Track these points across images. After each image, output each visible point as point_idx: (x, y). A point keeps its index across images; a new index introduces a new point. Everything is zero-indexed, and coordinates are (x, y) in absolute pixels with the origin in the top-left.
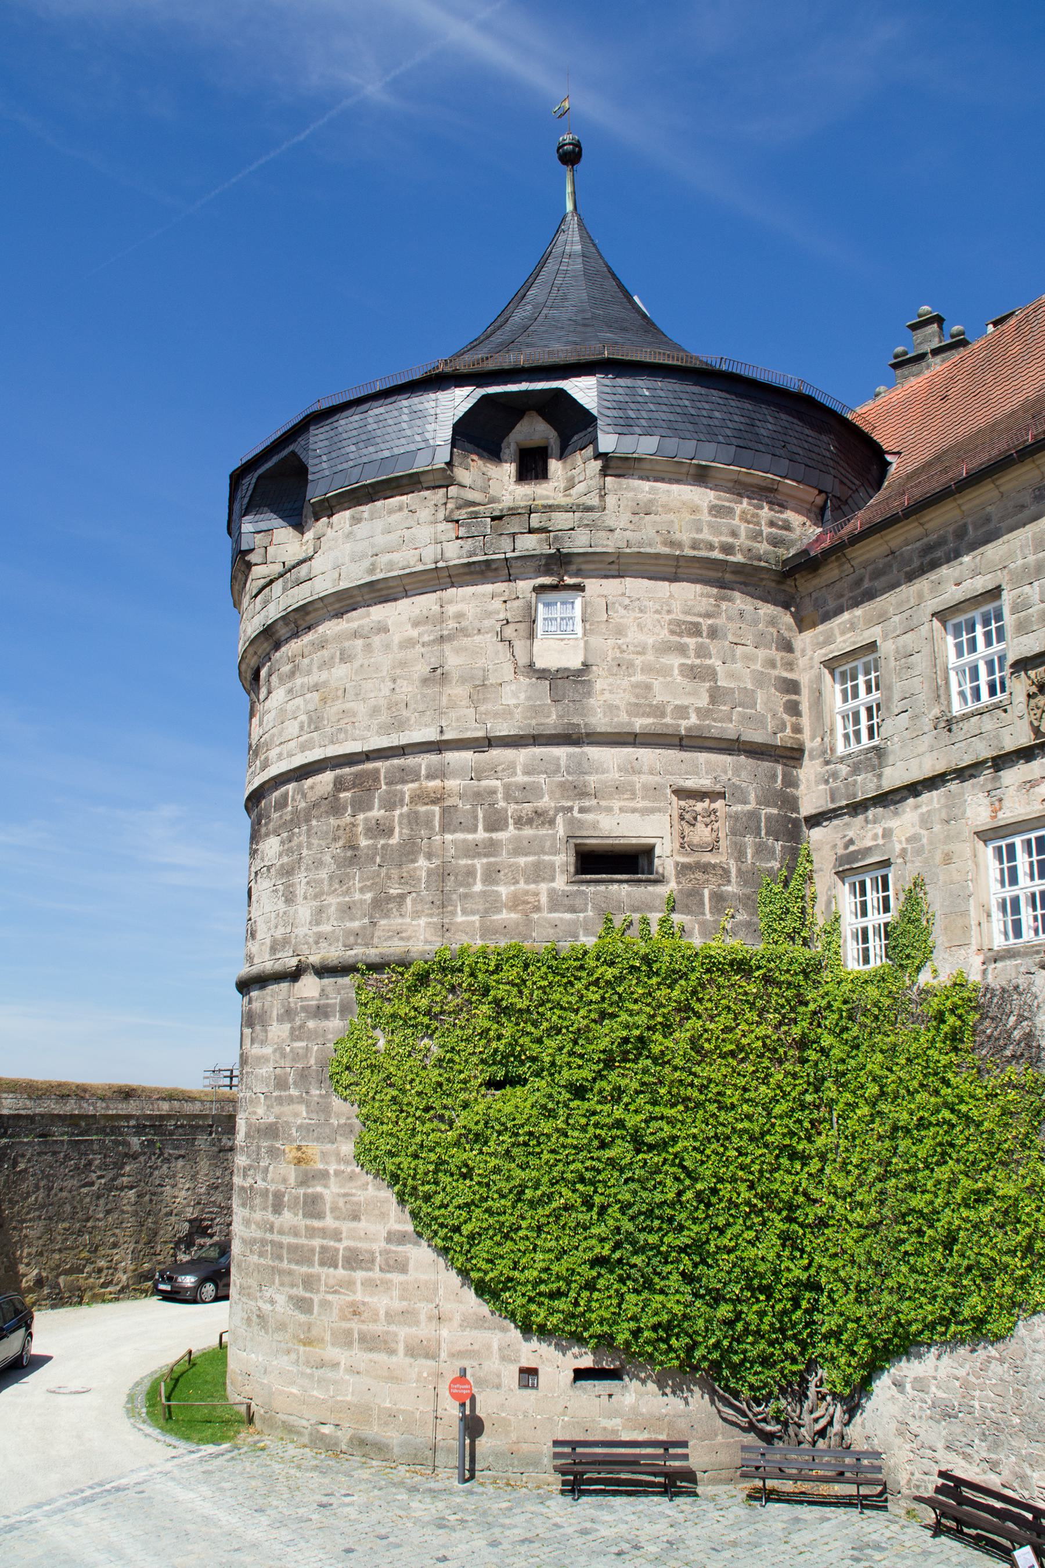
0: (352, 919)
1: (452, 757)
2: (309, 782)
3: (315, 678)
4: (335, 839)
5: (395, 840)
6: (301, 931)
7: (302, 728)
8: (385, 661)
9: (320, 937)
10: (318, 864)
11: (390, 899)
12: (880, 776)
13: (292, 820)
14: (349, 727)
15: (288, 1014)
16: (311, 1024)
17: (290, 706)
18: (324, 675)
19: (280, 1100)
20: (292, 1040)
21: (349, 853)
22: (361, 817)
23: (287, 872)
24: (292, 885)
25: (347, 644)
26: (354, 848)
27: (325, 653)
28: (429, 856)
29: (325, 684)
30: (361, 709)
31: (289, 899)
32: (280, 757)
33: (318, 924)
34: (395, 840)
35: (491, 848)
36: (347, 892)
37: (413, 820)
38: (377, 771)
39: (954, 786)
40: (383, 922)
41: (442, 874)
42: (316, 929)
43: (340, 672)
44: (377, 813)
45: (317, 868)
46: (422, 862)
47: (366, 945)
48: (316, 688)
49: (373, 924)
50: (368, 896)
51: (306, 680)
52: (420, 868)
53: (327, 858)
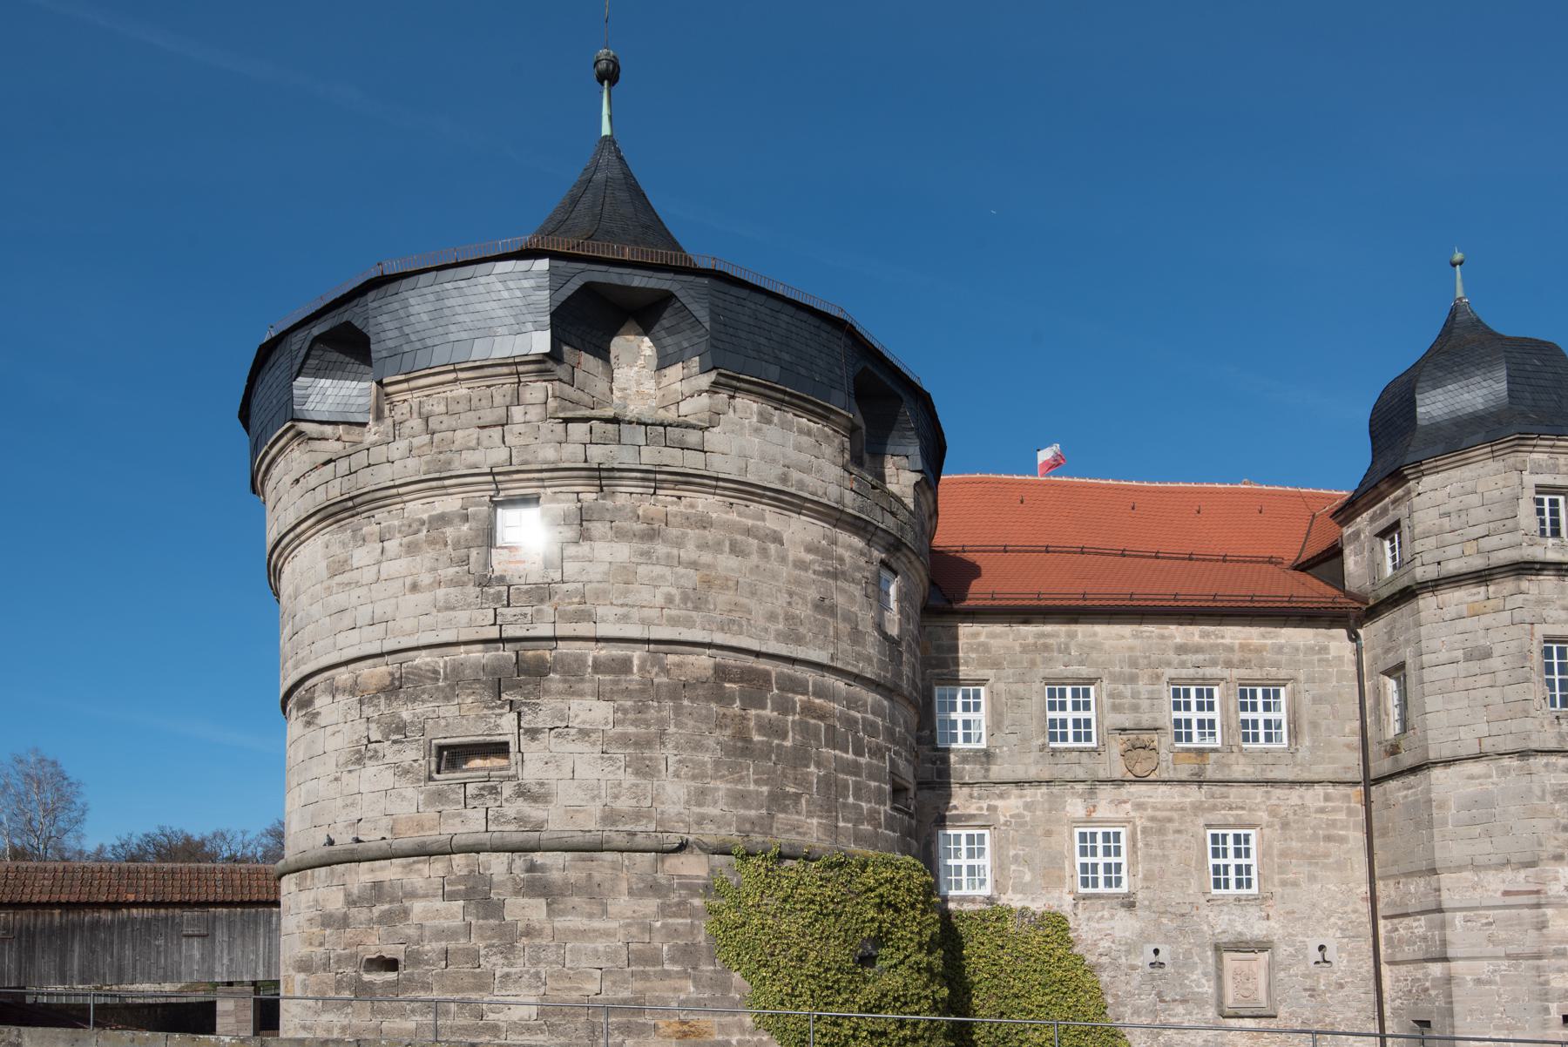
0: (748, 807)
1: (831, 680)
2: (671, 658)
3: (689, 552)
4: (720, 726)
5: (788, 743)
6: (672, 810)
7: (669, 599)
8: (785, 571)
9: (700, 821)
10: (699, 747)
11: (786, 795)
12: (987, 770)
13: (643, 691)
14: (744, 623)
15: (654, 889)
16: (697, 902)
17: (641, 570)
18: (706, 557)
19: (645, 976)
20: (664, 916)
21: (740, 744)
22: (753, 712)
23: (643, 743)
24: (651, 759)
25: (739, 537)
26: (748, 740)
27: (710, 535)
28: (818, 765)
29: (709, 566)
30: (758, 610)
31: (644, 769)
32: (625, 618)
33: (700, 805)
34: (788, 743)
35: (854, 769)
36: (740, 780)
37: (803, 728)
38: (767, 674)
39: (1056, 790)
40: (781, 816)
41: (827, 783)
42: (696, 810)
43: (726, 562)
44: (769, 713)
45: (694, 749)
46: (812, 769)
47: (765, 834)
48: (694, 565)
49: (771, 816)
50: (765, 789)
51: (675, 551)
52: (812, 774)
53: (711, 742)
